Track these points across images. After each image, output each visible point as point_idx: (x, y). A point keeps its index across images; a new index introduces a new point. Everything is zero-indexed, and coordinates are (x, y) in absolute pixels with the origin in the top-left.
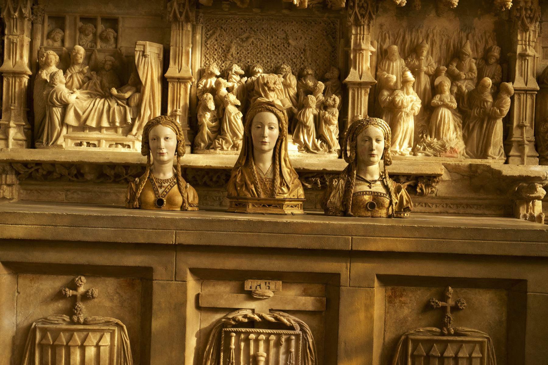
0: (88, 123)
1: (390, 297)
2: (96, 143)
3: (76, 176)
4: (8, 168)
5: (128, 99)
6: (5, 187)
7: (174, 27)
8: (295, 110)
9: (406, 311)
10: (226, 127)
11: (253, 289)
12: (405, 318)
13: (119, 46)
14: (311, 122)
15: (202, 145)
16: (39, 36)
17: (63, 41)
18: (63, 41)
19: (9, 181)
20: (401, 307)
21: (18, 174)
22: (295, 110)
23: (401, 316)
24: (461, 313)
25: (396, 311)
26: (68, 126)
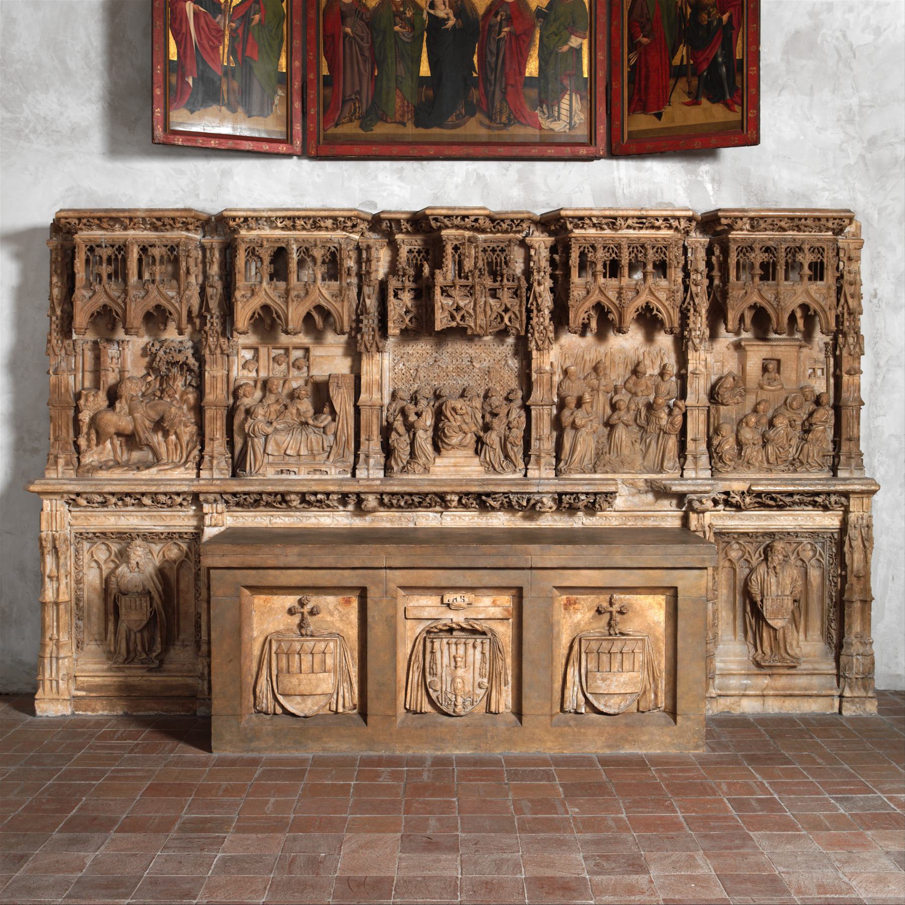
0: (288, 452)
1: (565, 605)
2: (296, 470)
3: (280, 503)
4: (218, 497)
5: (324, 428)
6: (215, 514)
7: (364, 358)
8: (482, 434)
9: (578, 617)
10: (418, 452)
11: (451, 602)
12: (579, 623)
13: (311, 374)
14: (497, 446)
15: (395, 468)
16: (235, 368)
17: (257, 371)
18: (257, 371)
19: (220, 510)
20: (575, 613)
21: (227, 502)
22: (482, 434)
23: (576, 621)
24: (625, 616)
25: (570, 617)
26: (268, 454)
